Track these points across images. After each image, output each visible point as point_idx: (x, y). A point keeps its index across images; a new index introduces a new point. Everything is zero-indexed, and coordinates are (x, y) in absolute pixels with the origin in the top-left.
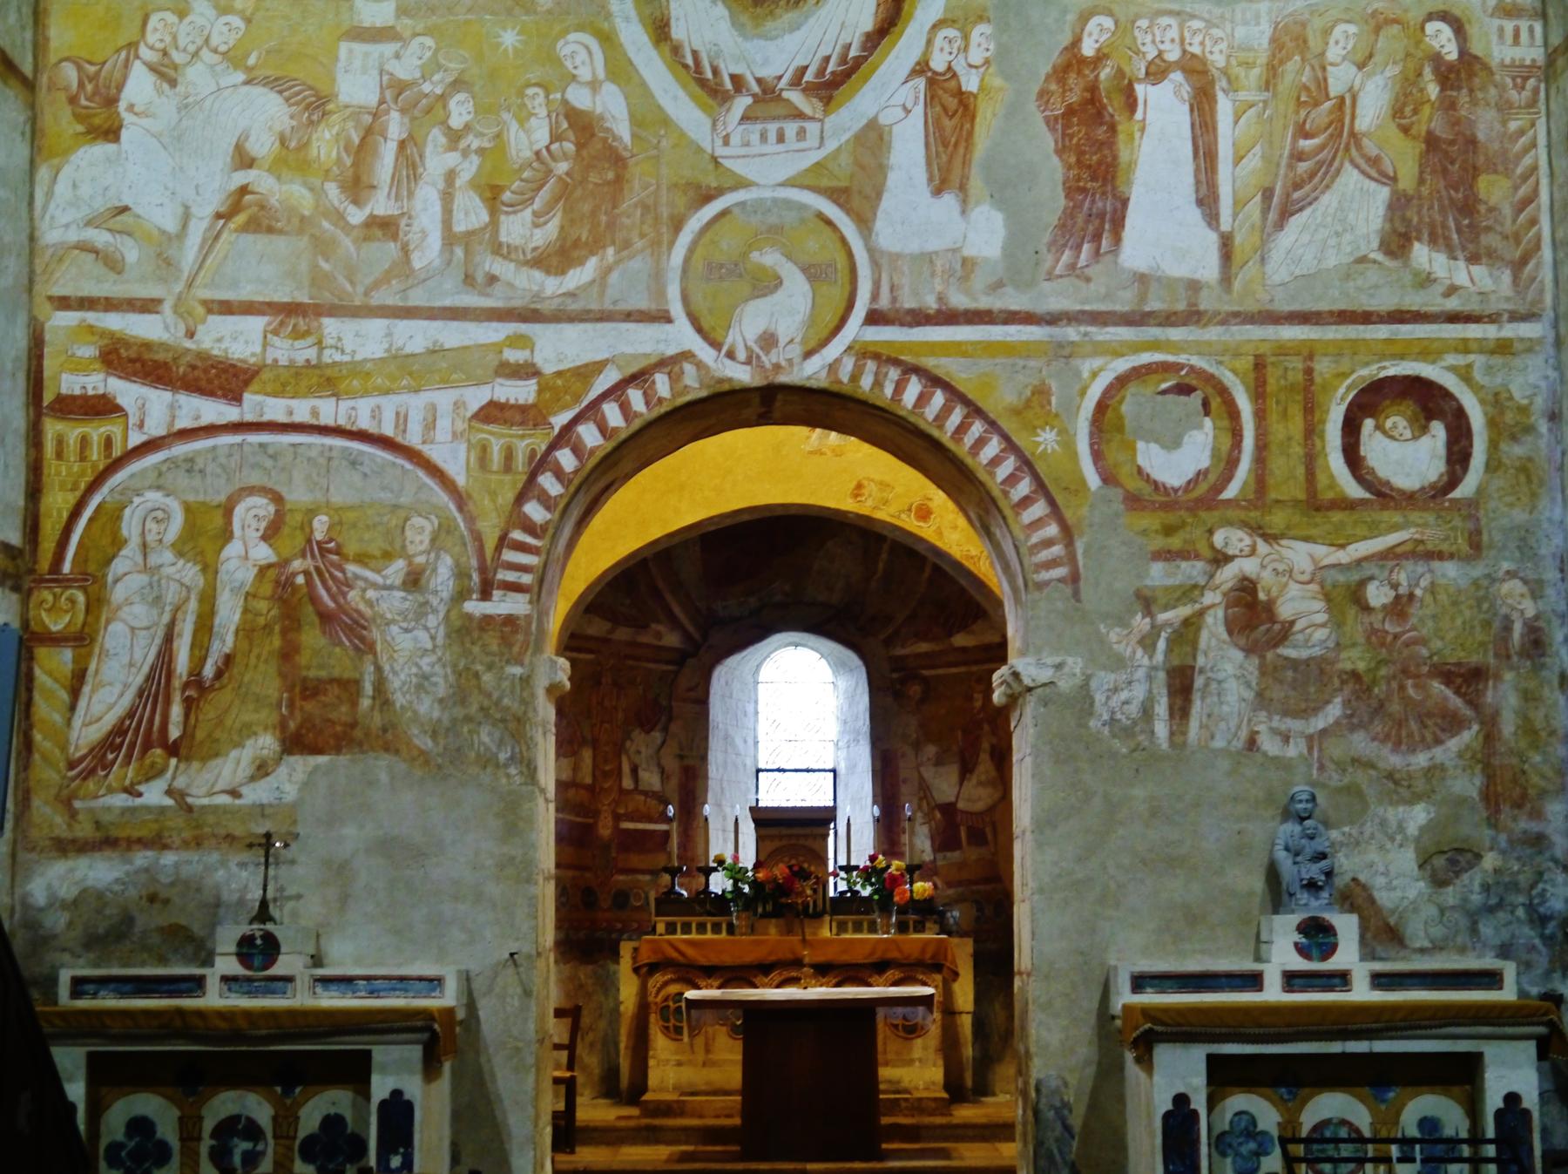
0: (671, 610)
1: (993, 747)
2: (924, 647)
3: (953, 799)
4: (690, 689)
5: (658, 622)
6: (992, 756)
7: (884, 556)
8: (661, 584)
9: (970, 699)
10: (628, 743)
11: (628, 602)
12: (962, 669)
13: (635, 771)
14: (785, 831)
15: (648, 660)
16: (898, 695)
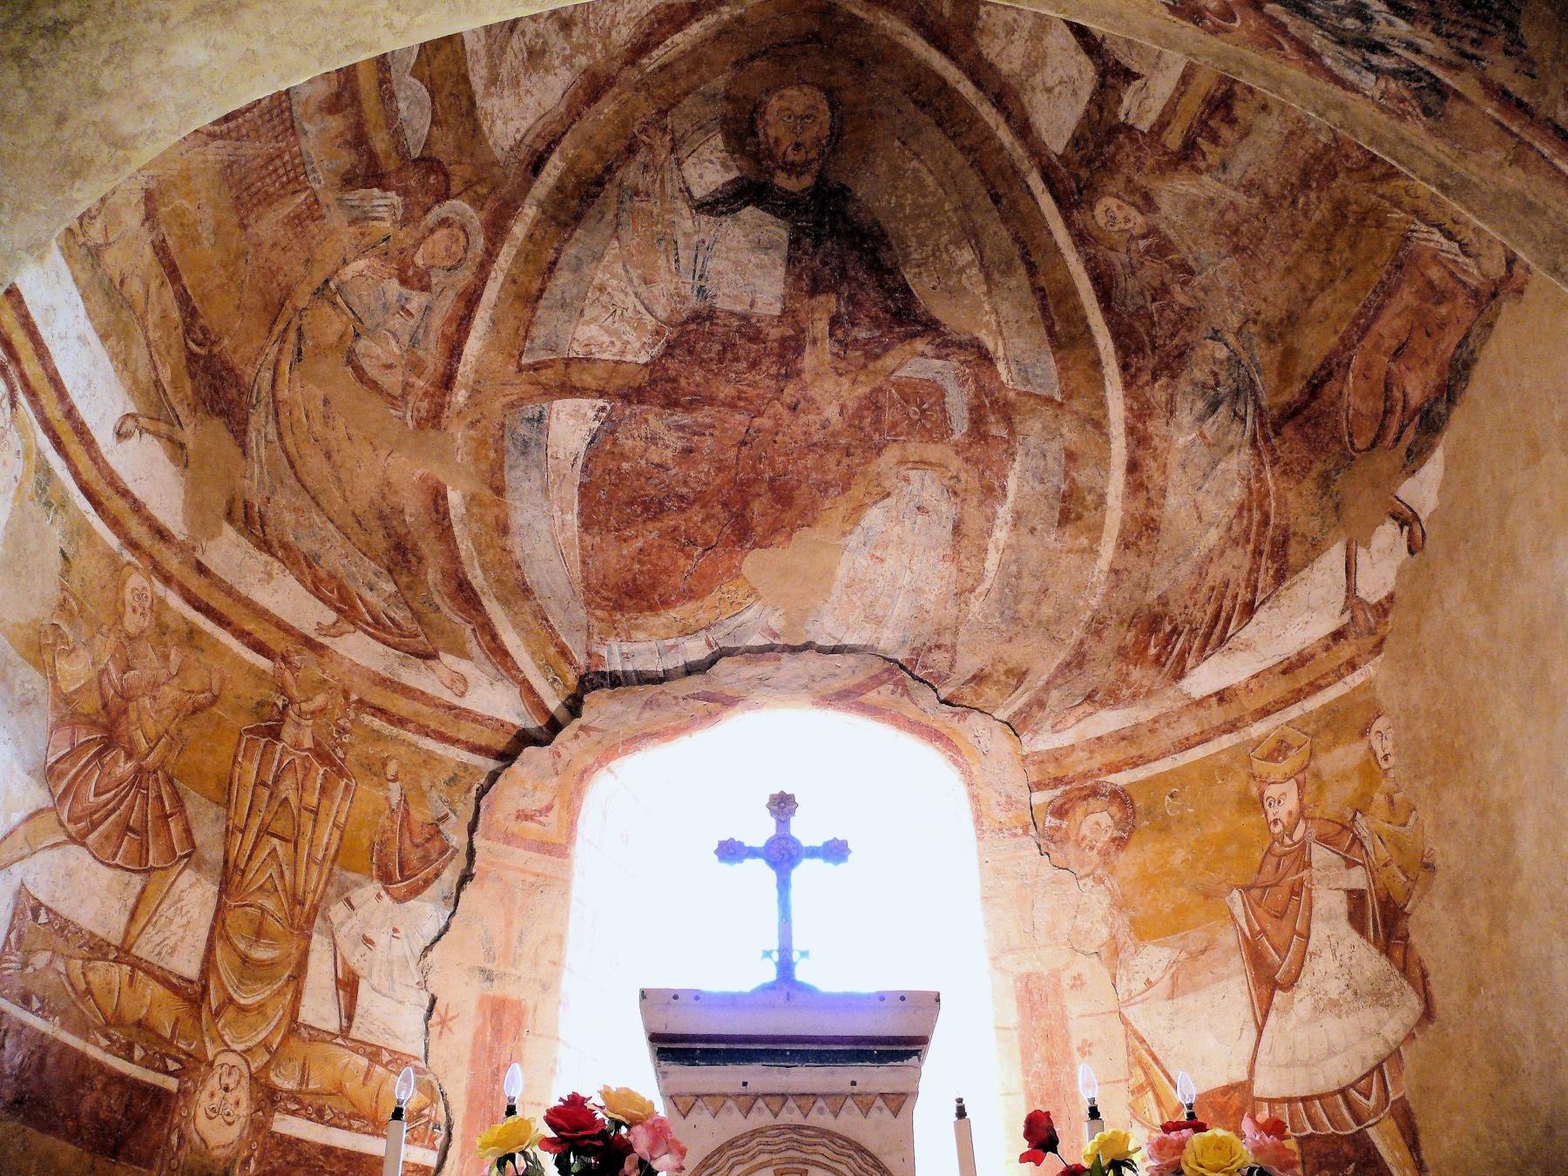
0: (494, 637)
1: (1356, 899)
2: (1110, 720)
3: (1240, 1075)
4: (523, 816)
5: (464, 654)
6: (1356, 918)
7: (1001, 535)
8: (477, 578)
9: (1258, 804)
10: (338, 911)
11: (390, 588)
12: (1227, 741)
13: (348, 985)
14: (760, 1077)
15: (424, 731)
16: (1049, 842)
